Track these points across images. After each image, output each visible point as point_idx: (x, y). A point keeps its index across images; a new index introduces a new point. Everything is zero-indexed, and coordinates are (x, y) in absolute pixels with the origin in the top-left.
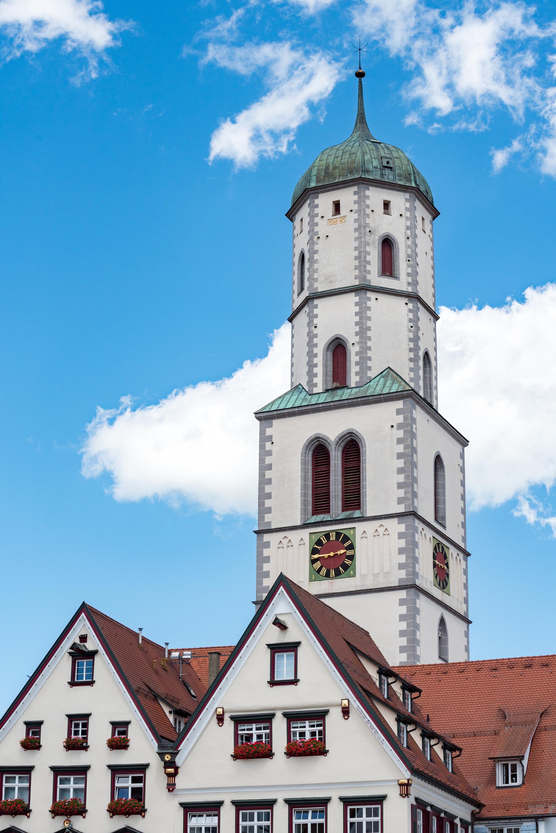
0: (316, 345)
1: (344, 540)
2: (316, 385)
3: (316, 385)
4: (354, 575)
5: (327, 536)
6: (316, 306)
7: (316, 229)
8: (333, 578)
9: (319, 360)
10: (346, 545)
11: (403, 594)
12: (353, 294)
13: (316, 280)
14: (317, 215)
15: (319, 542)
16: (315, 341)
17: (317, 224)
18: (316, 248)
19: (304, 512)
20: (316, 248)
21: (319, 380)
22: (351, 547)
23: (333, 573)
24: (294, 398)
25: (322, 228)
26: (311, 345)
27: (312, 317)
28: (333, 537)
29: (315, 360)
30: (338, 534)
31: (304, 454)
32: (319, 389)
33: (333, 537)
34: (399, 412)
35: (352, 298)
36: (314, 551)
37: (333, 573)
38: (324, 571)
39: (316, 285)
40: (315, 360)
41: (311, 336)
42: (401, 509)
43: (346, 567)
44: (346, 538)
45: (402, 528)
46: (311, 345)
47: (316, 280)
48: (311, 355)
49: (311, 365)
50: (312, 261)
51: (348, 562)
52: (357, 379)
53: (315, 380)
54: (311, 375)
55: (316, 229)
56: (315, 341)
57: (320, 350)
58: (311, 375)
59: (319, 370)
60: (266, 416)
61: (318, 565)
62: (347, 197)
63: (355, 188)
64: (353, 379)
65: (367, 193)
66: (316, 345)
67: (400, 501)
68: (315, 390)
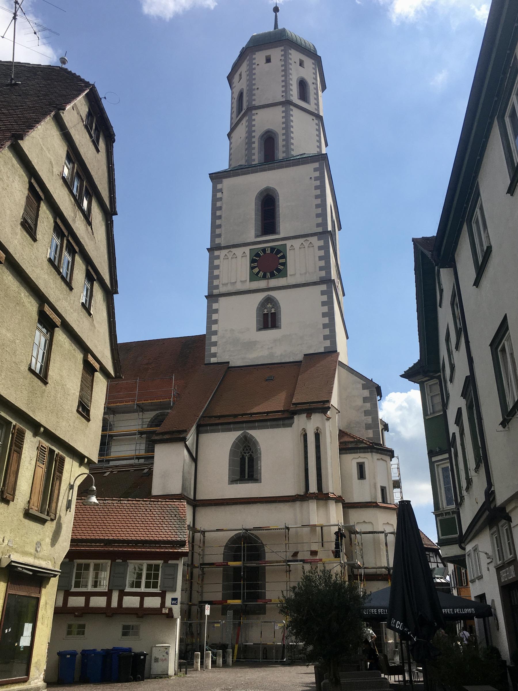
2: (254, 160)
3: (254, 160)
5: (264, 250)
8: (269, 279)
9: (256, 145)
10: (279, 256)
11: (324, 287)
12: (281, 106)
15: (257, 255)
17: (255, 69)
23: (268, 275)
27: (250, 121)
28: (268, 251)
30: (272, 249)
33: (268, 251)
34: (315, 170)
35: (281, 109)
37: (268, 275)
38: (261, 274)
42: (320, 230)
43: (279, 271)
44: (279, 252)
45: (321, 243)
52: (284, 155)
56: (253, 134)
57: (256, 140)
59: (256, 151)
60: (216, 177)
62: (276, 53)
63: (282, 48)
64: (280, 155)
65: (290, 51)
67: (318, 225)
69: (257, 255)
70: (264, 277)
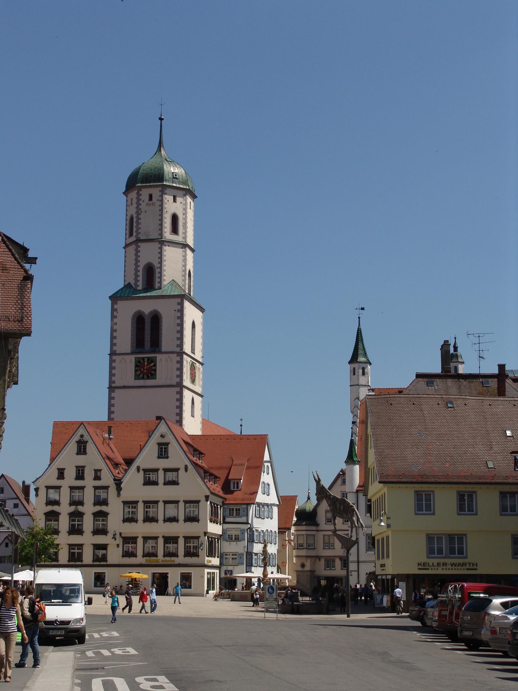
0: (139, 266)
1: (153, 361)
2: (139, 286)
3: (139, 286)
4: (156, 379)
5: (143, 359)
6: (139, 247)
7: (140, 207)
8: (145, 379)
9: (140, 273)
13: (140, 233)
14: (141, 200)
16: (139, 264)
17: (141, 204)
18: (140, 216)
19: (132, 347)
20: (140, 216)
21: (140, 283)
22: (155, 365)
23: (145, 377)
24: (128, 291)
25: (143, 206)
26: (137, 266)
27: (137, 251)
29: (139, 273)
30: (148, 358)
31: (133, 319)
32: (140, 288)
36: (136, 366)
37: (145, 377)
38: (141, 376)
39: (140, 236)
40: (139, 273)
41: (137, 261)
43: (152, 374)
46: (137, 266)
47: (140, 233)
48: (137, 271)
49: (137, 276)
50: (138, 223)
51: (153, 372)
53: (138, 283)
54: (136, 281)
55: (140, 207)
56: (139, 264)
57: (141, 269)
58: (136, 281)
59: (140, 278)
61: (139, 372)
66: (139, 266)
68: (139, 288)
69: (139, 362)
70: (143, 378)
